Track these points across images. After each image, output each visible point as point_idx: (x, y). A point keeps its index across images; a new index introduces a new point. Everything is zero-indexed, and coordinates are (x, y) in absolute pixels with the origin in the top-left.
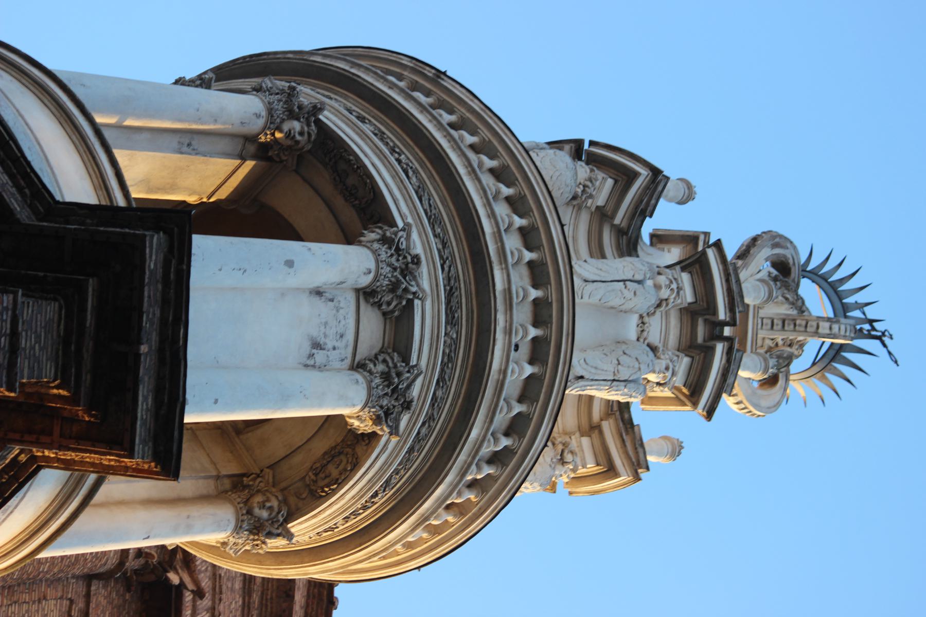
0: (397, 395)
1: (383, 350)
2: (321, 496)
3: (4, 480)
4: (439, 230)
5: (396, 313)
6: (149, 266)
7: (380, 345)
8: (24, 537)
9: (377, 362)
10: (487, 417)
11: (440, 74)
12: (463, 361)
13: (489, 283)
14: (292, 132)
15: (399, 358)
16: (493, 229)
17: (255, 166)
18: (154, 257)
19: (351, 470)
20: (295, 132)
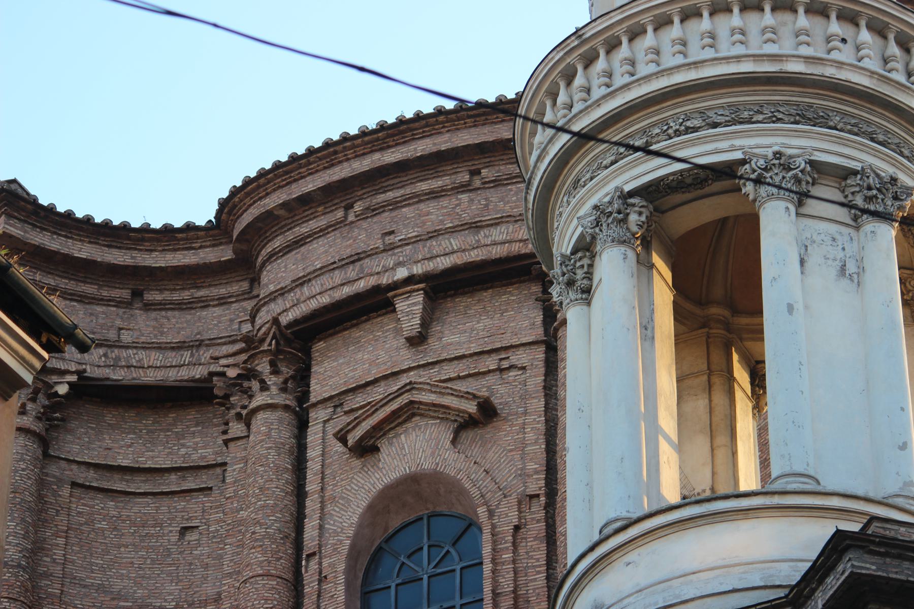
0: (883, 189)
1: (842, 189)
4: (746, 113)
5: (816, 176)
6: (874, 571)
7: (837, 191)
9: (854, 202)
10: (904, 91)
11: (577, 33)
12: (856, 108)
13: (798, 77)
14: (639, 223)
15: (853, 179)
16: (750, 60)
17: (655, 252)
18: (868, 566)
20: (639, 220)
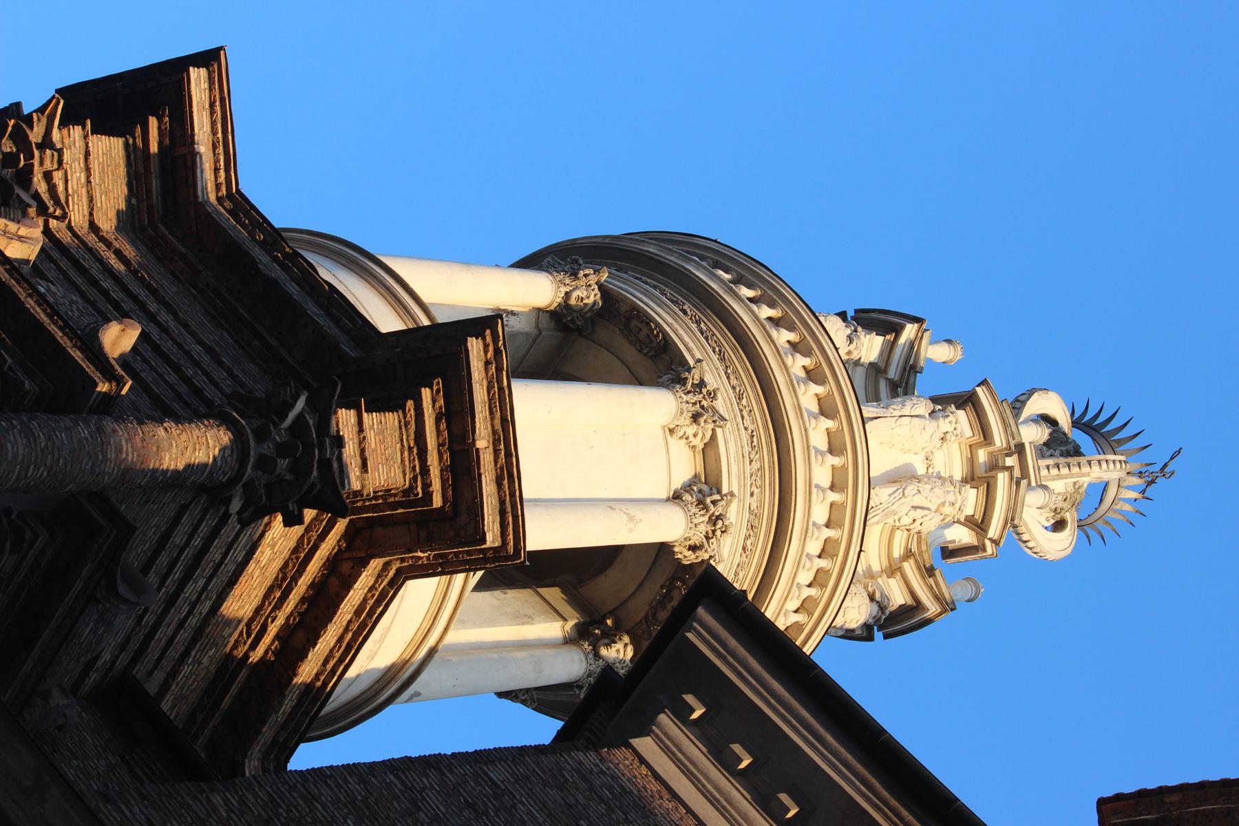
2: (664, 337)
3: (247, 221)
8: (401, 310)
19: (638, 312)
